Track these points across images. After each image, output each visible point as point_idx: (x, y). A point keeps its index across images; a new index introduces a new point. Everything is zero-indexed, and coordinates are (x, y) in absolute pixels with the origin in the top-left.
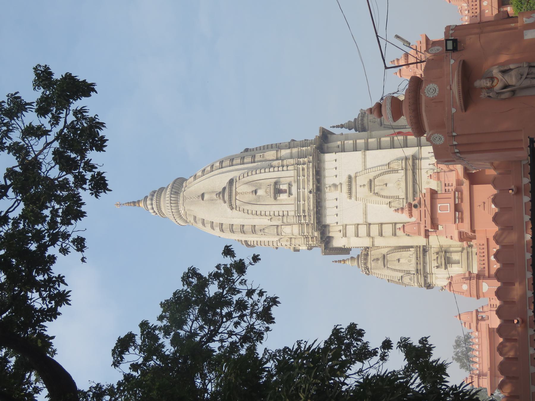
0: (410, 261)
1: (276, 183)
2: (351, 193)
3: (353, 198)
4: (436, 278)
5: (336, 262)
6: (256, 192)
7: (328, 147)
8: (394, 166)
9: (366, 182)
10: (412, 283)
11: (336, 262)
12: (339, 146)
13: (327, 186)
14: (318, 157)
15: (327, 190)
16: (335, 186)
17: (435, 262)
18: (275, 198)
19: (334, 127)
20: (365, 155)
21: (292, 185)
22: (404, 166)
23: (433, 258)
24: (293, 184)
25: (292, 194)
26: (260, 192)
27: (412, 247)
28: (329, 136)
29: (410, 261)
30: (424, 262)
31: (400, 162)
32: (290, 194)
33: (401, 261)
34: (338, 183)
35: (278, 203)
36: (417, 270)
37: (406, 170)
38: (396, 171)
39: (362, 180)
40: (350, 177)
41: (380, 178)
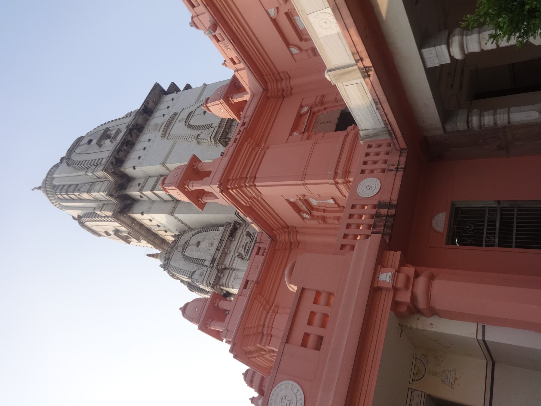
0: (211, 245)
4: (236, 278)
5: (149, 255)
10: (200, 280)
11: (149, 255)
16: (157, 125)
17: (243, 250)
21: (121, 131)
23: (242, 244)
25: (115, 140)
26: (94, 142)
27: (222, 225)
29: (211, 245)
30: (227, 247)
33: (202, 245)
35: (101, 149)
36: (214, 260)
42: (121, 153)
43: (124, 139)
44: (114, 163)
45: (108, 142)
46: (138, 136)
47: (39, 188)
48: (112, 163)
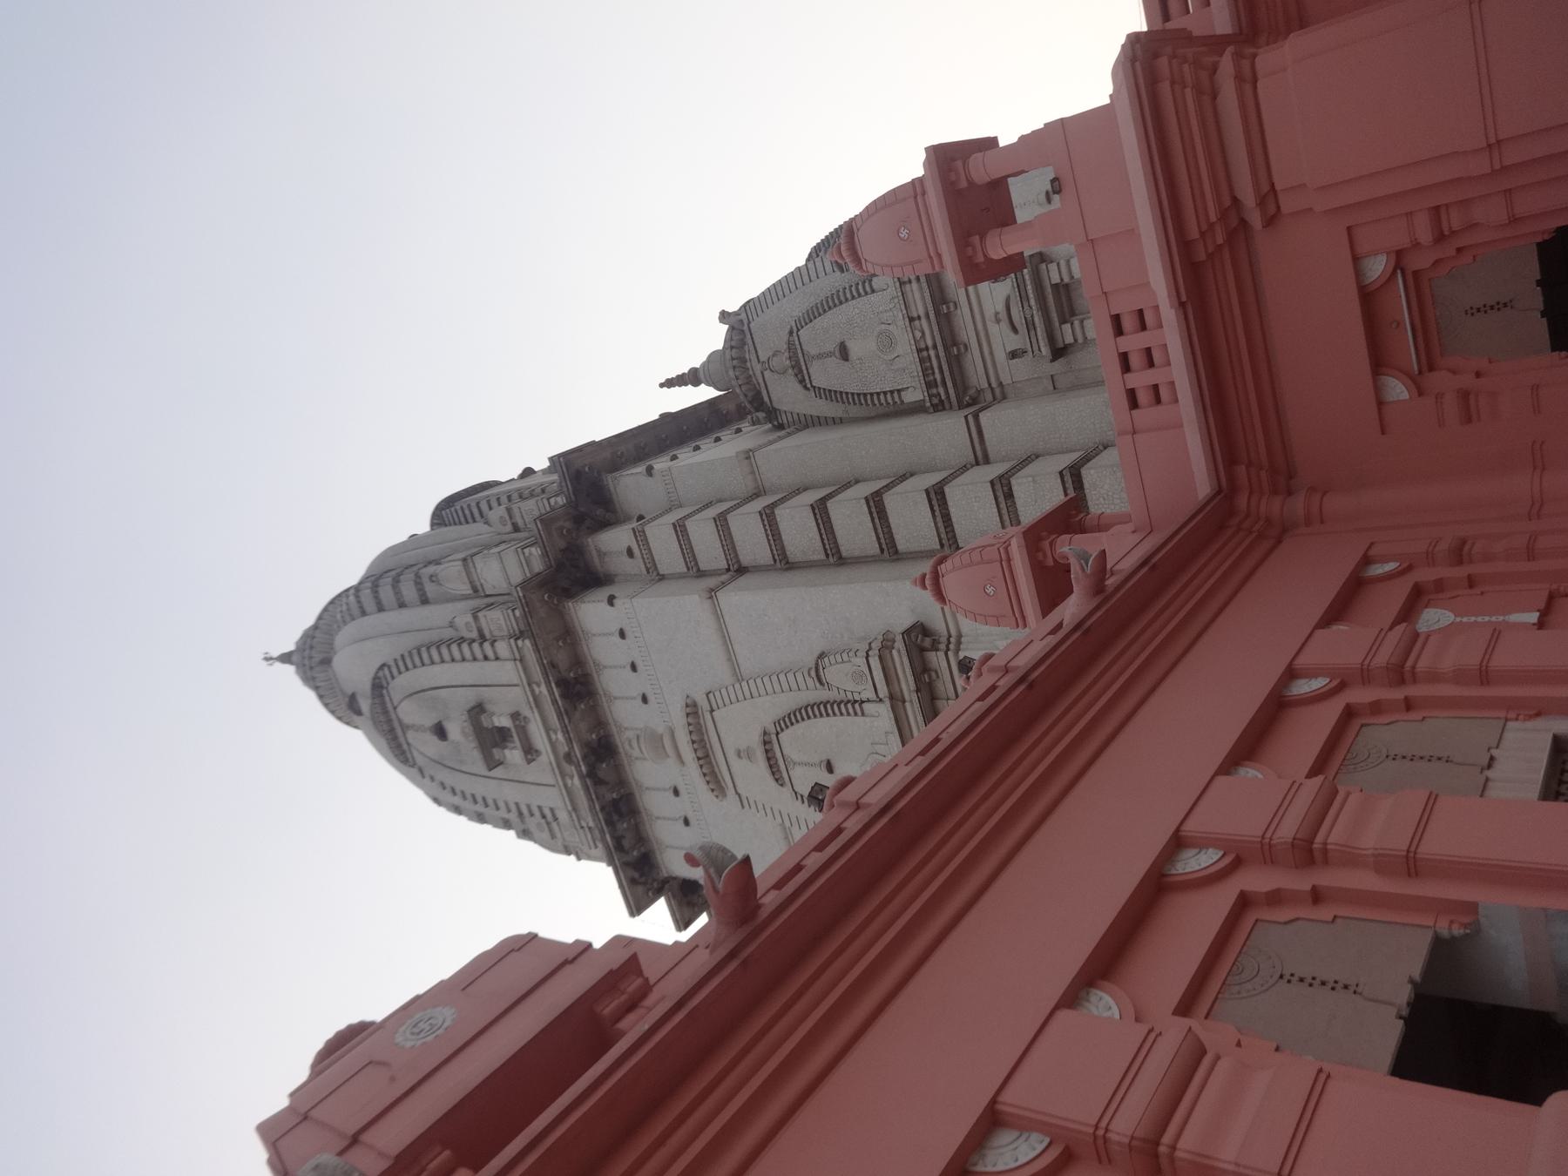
1: (477, 711)
2: (713, 773)
3: (730, 792)
6: (440, 731)
7: (602, 554)
8: (842, 678)
9: (755, 739)
12: (630, 553)
13: (630, 734)
14: (560, 615)
15: (636, 753)
18: (492, 764)
19: (669, 383)
20: (718, 616)
22: (883, 691)
24: (526, 712)
26: (455, 730)
28: (609, 479)
31: (861, 661)
32: (530, 752)
34: (660, 730)
37: (896, 700)
38: (853, 705)
39: (738, 727)
40: (692, 710)
41: (799, 729)
42: (626, 843)
43: (602, 809)
44: (636, 875)
45: (514, 755)
46: (618, 769)
47: (285, 658)
48: (633, 882)
